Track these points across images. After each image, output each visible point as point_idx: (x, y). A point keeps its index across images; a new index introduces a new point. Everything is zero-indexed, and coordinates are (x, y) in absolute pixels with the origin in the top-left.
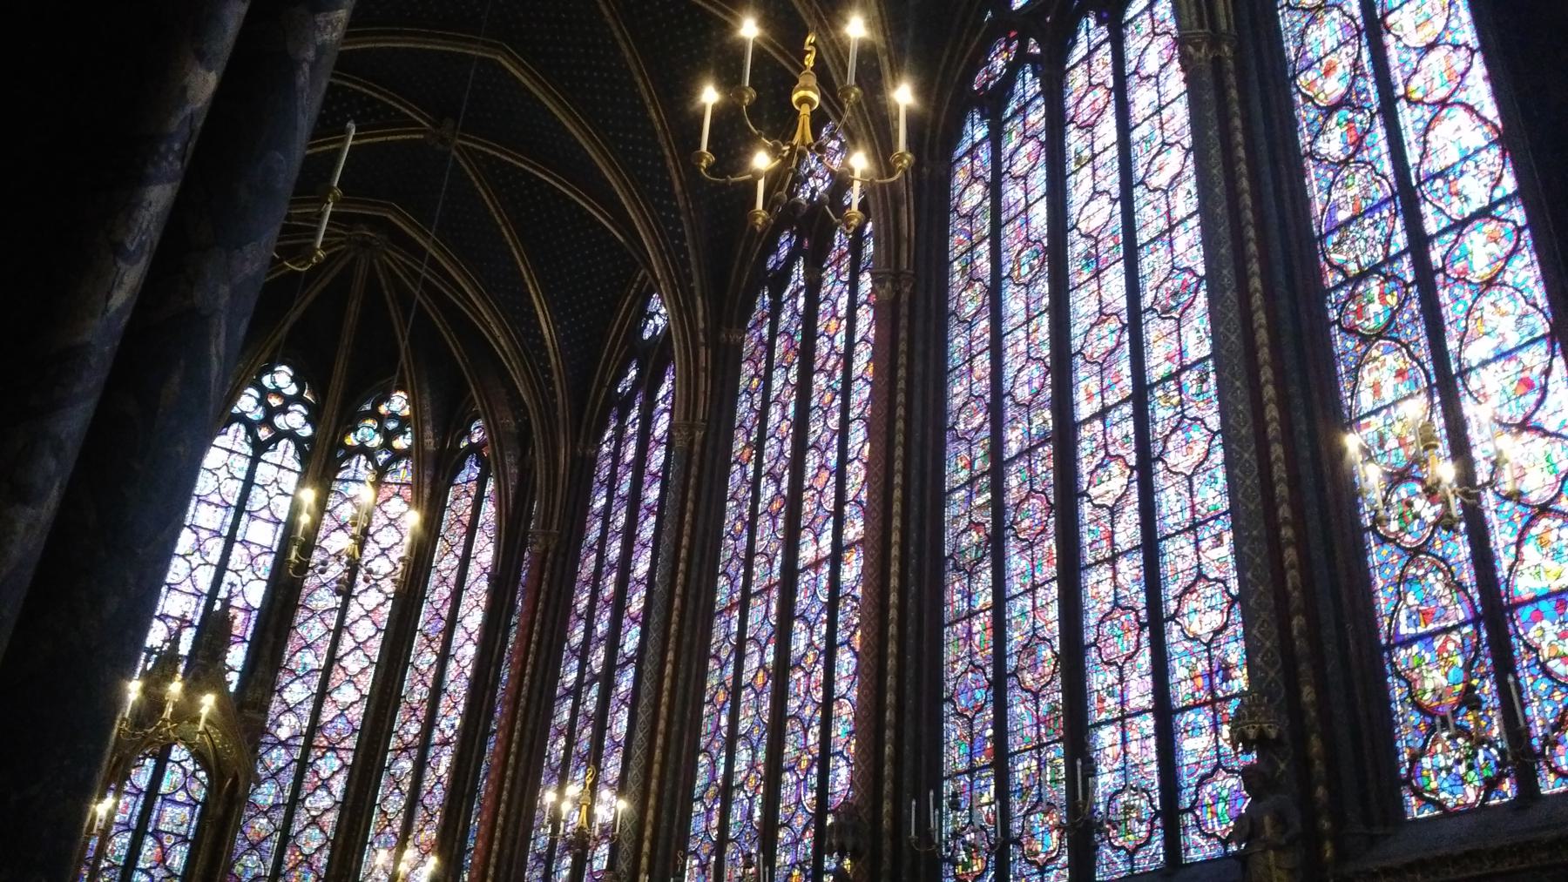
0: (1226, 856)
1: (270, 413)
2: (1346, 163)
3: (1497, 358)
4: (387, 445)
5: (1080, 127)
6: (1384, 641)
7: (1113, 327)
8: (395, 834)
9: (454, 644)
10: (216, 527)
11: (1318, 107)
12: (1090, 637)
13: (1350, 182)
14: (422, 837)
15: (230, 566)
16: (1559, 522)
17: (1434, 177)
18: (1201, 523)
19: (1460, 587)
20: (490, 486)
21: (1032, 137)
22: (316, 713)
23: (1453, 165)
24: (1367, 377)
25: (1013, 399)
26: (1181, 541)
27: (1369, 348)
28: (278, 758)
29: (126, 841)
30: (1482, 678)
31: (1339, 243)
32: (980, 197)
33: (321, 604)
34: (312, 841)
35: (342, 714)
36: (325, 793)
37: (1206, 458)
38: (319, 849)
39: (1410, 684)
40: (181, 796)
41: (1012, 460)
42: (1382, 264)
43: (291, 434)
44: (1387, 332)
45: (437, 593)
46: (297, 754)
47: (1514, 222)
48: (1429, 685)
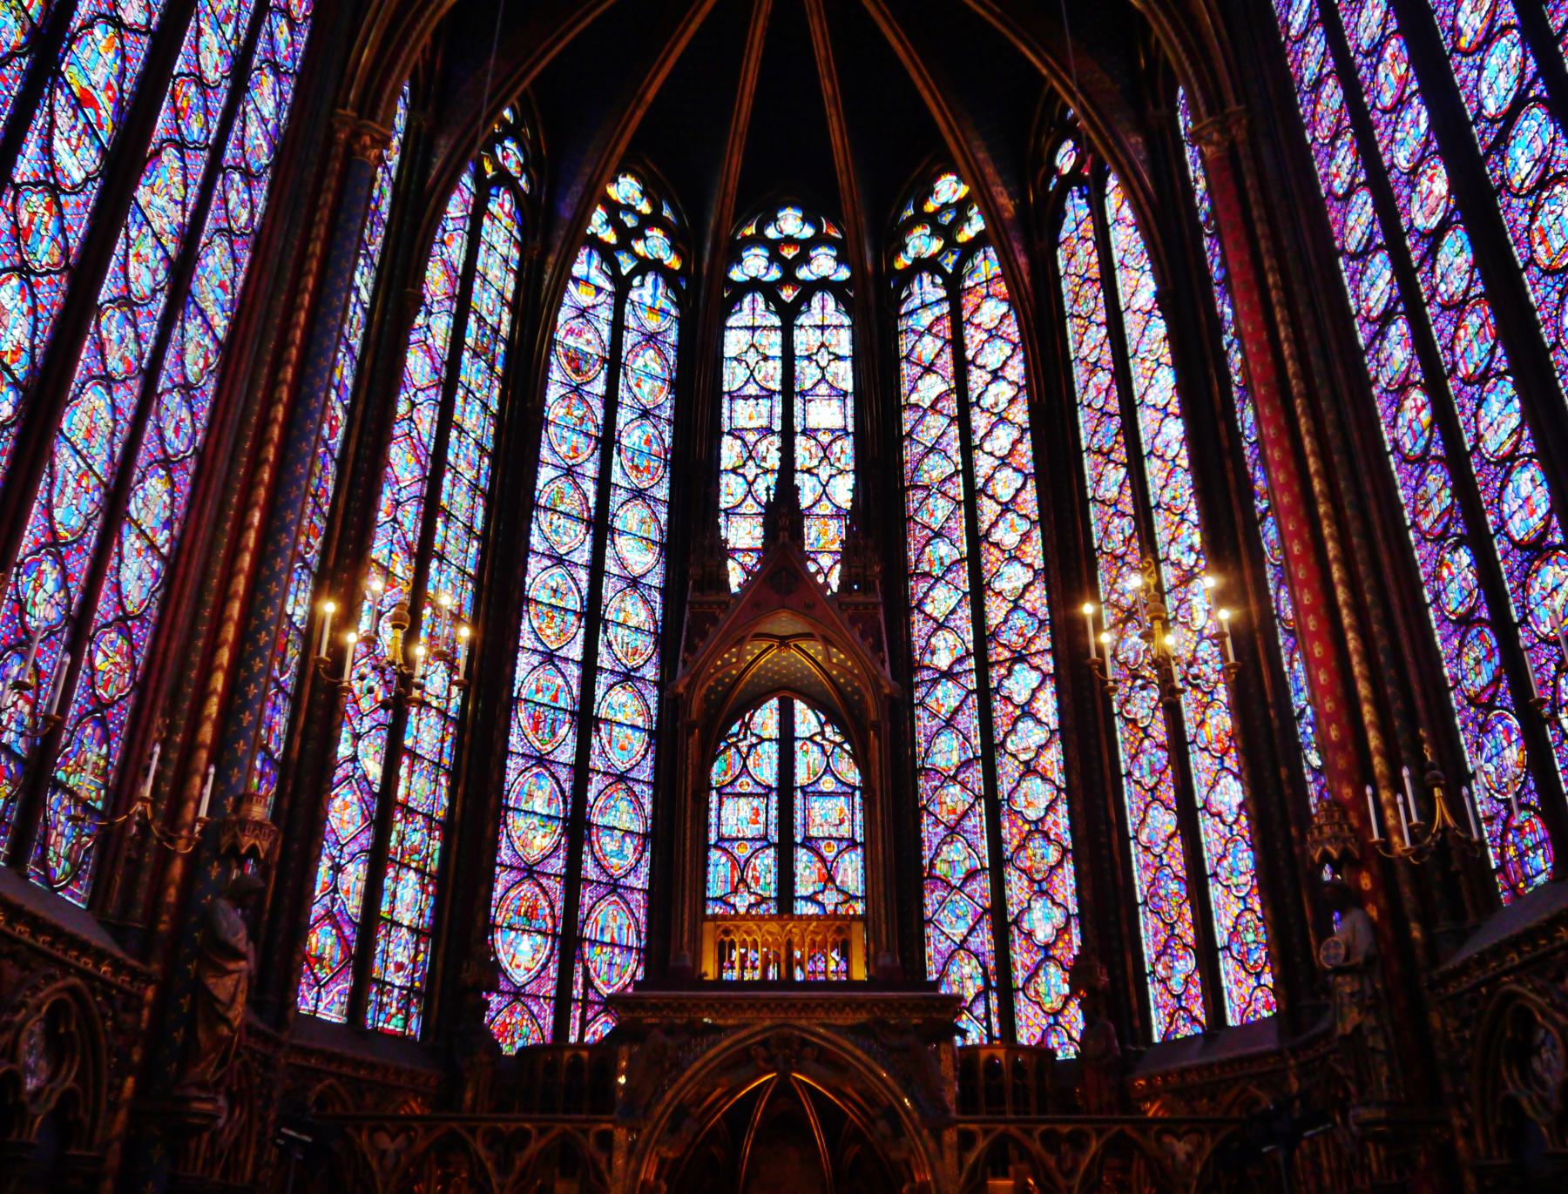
1: (789, 268)
4: (950, 244)
8: (1160, 746)
9: (1144, 437)
10: (764, 422)
14: (1209, 731)
15: (798, 466)
20: (1115, 201)
22: (979, 617)
28: (946, 696)
29: (770, 861)
33: (934, 474)
34: (1035, 797)
35: (1016, 607)
36: (1031, 724)
38: (1050, 808)
40: (828, 784)
43: (824, 284)
45: (1092, 387)
46: (971, 682)
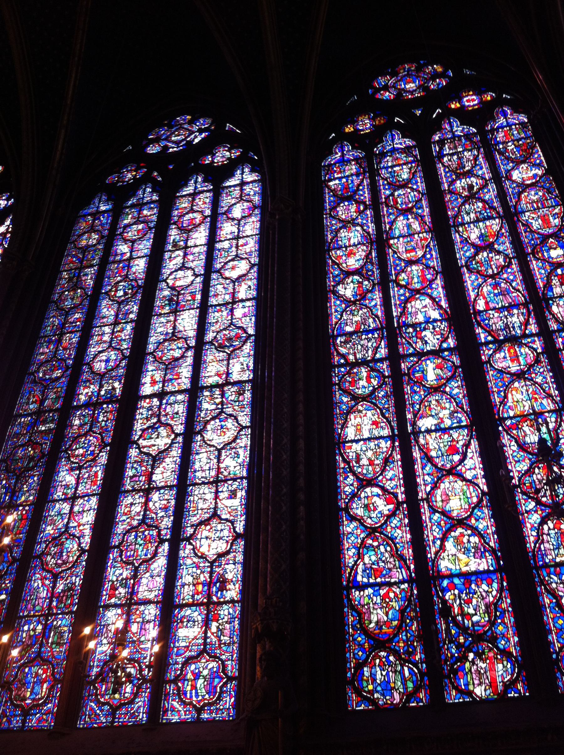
0: (198, 720)
2: (354, 303)
3: (436, 431)
5: (179, 228)
6: (344, 583)
7: (180, 345)
11: (341, 270)
12: (115, 541)
13: (356, 313)
16: (469, 532)
17: (409, 326)
18: (222, 481)
19: (401, 558)
21: (142, 222)
23: (420, 323)
24: (353, 420)
25: (91, 368)
26: (205, 489)
27: (357, 404)
30: (411, 620)
31: (346, 342)
32: (95, 241)
37: (234, 440)
39: (360, 614)
41: (79, 407)
42: (370, 361)
44: (369, 398)
47: (453, 362)
48: (374, 618)
